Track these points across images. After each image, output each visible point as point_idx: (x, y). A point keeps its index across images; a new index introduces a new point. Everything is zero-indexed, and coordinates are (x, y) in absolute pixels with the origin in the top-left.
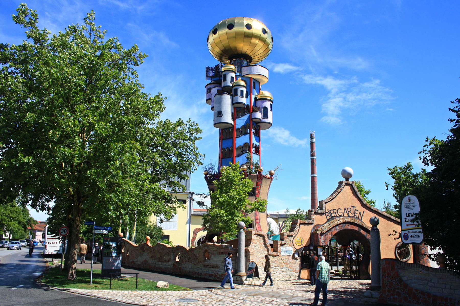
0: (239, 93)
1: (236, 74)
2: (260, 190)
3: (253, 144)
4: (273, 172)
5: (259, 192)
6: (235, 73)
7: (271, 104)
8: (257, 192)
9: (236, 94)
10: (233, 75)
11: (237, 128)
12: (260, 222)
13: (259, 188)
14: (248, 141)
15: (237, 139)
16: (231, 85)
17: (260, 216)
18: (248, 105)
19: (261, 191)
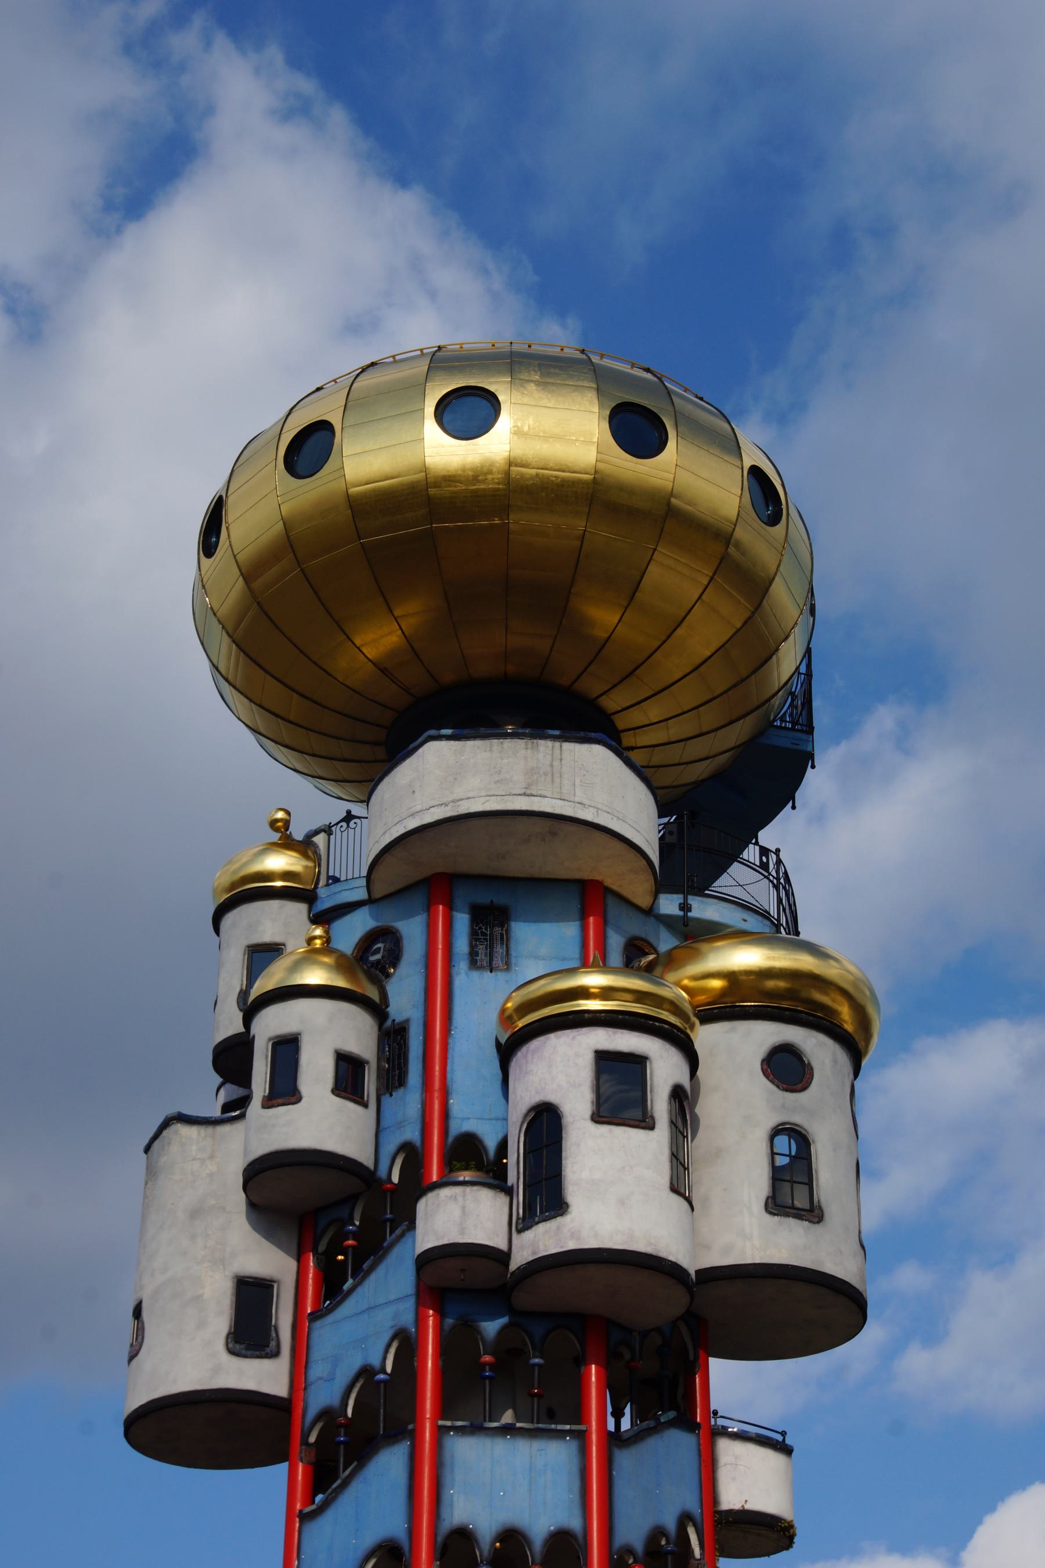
1: (324, 904)
3: (463, 1535)
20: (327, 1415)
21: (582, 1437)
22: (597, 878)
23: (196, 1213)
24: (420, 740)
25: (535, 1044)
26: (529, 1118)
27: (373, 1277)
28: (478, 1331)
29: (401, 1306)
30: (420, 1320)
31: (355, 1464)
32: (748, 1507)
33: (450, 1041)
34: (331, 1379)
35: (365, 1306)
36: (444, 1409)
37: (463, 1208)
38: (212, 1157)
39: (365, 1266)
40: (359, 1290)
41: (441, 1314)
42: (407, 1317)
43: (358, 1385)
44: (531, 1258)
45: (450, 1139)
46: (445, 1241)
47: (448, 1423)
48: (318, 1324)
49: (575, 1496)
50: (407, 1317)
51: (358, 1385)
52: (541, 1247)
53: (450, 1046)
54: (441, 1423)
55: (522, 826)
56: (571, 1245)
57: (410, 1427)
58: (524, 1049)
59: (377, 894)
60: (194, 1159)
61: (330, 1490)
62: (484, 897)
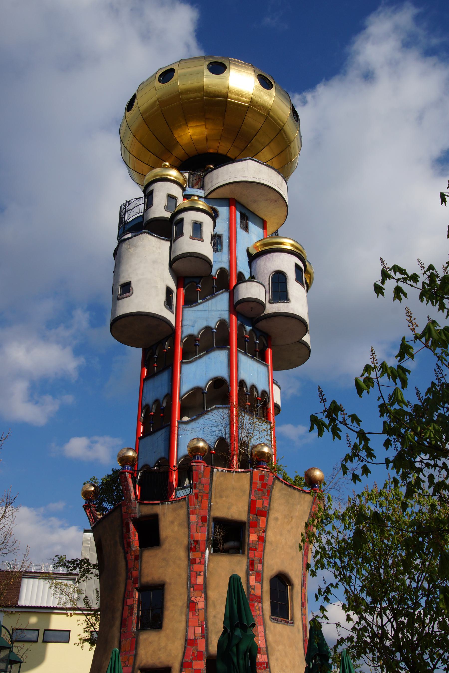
0: (188, 229)
1: (186, 193)
2: (264, 531)
3: (242, 383)
4: (318, 474)
5: (262, 539)
6: (184, 190)
7: (297, 266)
8: (253, 537)
9: (180, 233)
10: (177, 191)
11: (185, 334)
12: (273, 664)
13: (262, 525)
14: (223, 373)
15: (185, 367)
16: (168, 215)
17: (270, 638)
18: (222, 270)
19: (270, 535)
20: (191, 337)
21: (268, 366)
22: (267, 221)
23: (155, 262)
24: (247, 158)
25: (269, 256)
26: (273, 273)
27: (207, 302)
28: (245, 328)
29: (222, 312)
30: (230, 318)
31: (205, 352)
32: (277, 403)
33: (237, 245)
34: (193, 326)
35: (207, 309)
36: (239, 346)
37: (260, 290)
38: (159, 248)
39: (207, 298)
40: (204, 304)
41: (238, 318)
42: (226, 315)
43: (203, 331)
44: (277, 311)
45: (238, 272)
46: (255, 297)
47: (240, 350)
48: (187, 309)
49: (267, 382)
50: (226, 315)
51: (203, 331)
52: (282, 309)
53: (237, 246)
54: (238, 349)
55: (273, 196)
56: (291, 312)
57: (229, 347)
58: (271, 254)
59: (209, 197)
60: (153, 246)
61: (194, 357)
62: (244, 211)
